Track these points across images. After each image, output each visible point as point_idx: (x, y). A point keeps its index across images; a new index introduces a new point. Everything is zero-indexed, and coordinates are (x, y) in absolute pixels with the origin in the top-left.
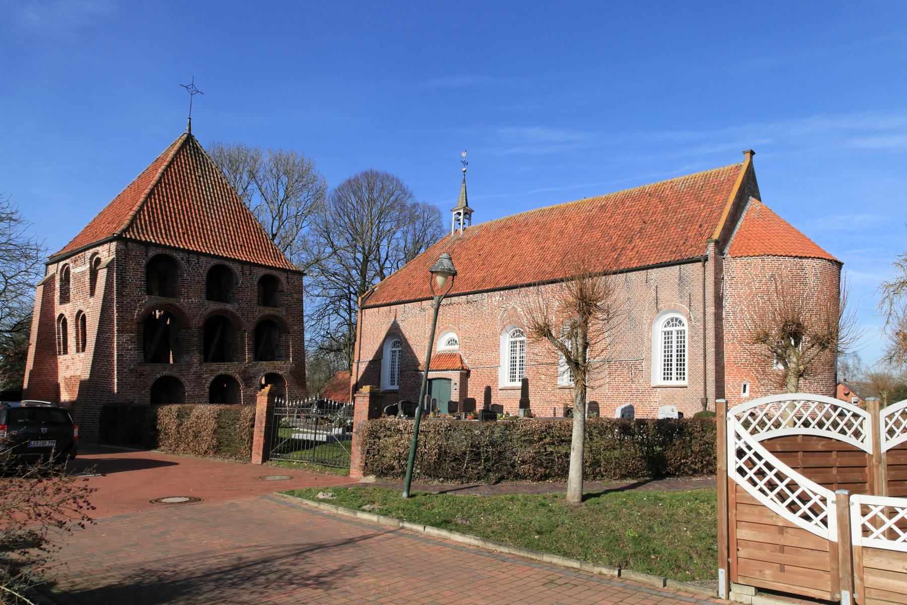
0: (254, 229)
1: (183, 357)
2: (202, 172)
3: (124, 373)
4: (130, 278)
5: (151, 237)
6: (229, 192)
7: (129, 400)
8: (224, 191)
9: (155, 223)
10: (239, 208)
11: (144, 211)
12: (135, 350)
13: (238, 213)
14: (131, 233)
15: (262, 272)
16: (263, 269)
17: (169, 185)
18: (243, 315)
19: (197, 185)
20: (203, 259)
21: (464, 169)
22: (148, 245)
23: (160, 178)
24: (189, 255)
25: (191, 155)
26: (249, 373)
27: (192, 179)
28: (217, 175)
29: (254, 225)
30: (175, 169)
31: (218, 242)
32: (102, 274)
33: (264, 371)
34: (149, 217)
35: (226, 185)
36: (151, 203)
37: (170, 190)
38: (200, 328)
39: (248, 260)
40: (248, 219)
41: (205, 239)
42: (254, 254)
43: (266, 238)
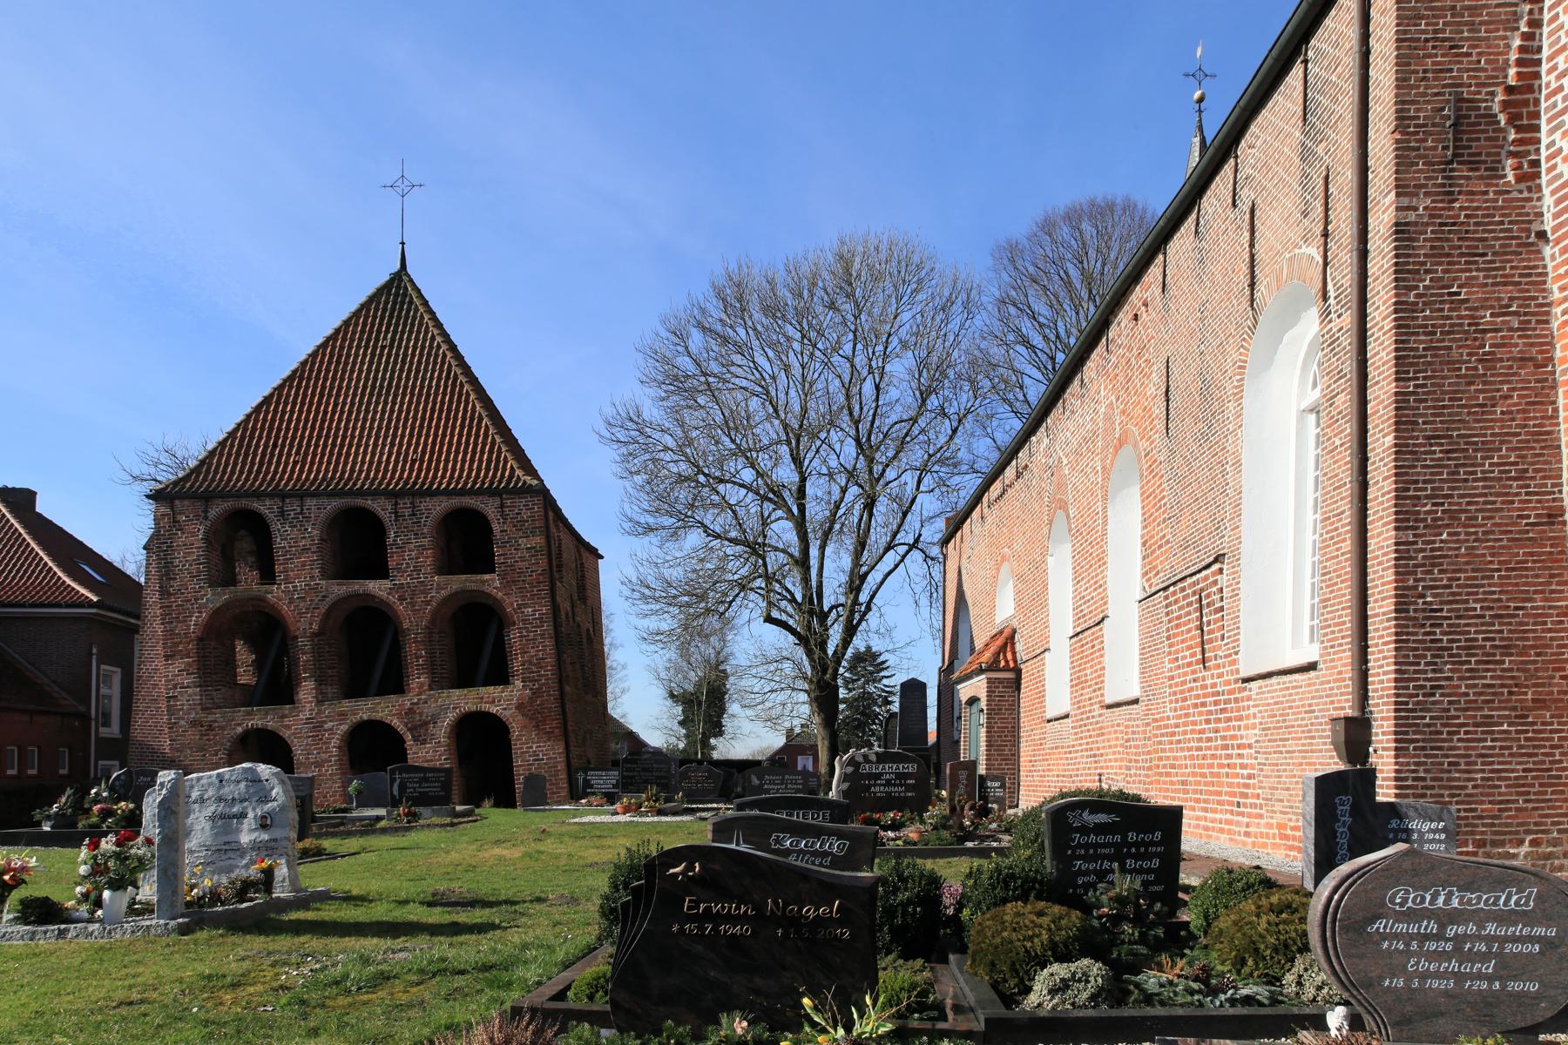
15: (439, 506)
16: (441, 498)
18: (402, 599)
21: (1197, 95)
22: (207, 498)
24: (283, 501)
33: (455, 708)
38: (314, 635)
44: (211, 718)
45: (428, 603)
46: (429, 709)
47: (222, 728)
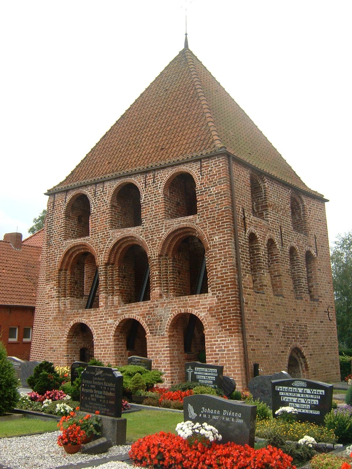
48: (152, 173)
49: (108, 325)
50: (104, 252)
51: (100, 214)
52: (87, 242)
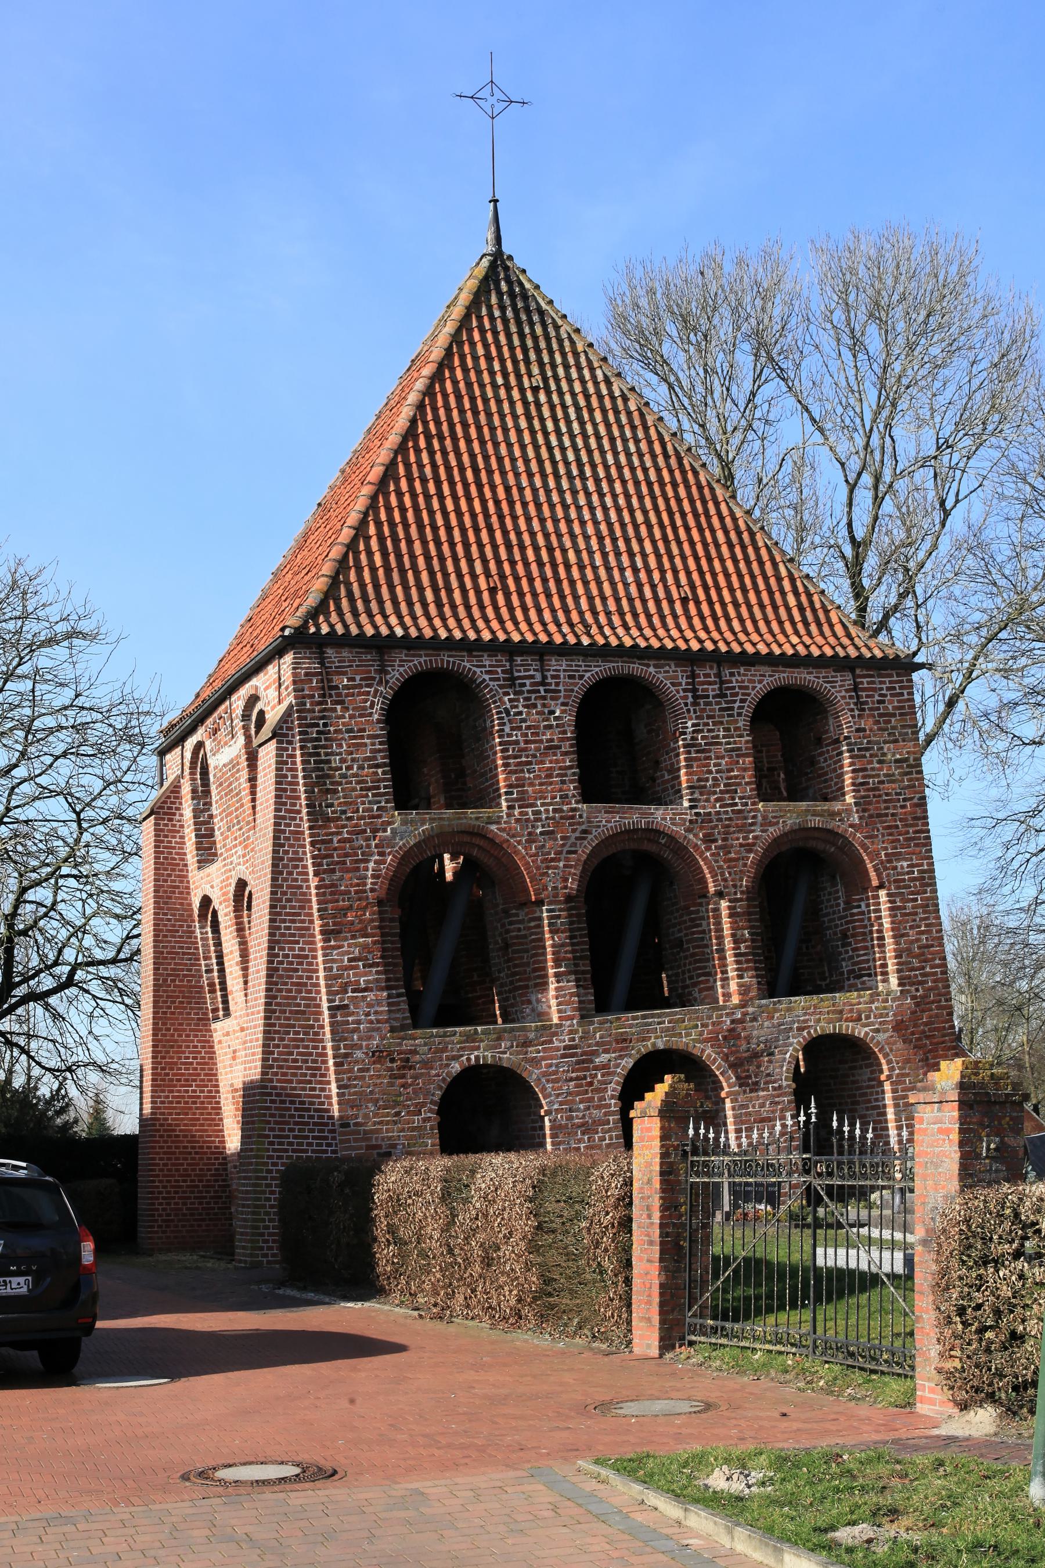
0: (726, 533)
1: (529, 1002)
2: (543, 373)
3: (357, 1062)
4: (343, 761)
5: (393, 620)
6: (637, 422)
7: (379, 1147)
8: (618, 421)
9: (403, 572)
10: (671, 472)
11: (368, 538)
12: (382, 989)
13: (669, 489)
14: (334, 618)
17: (441, 438)
18: (709, 839)
19: (529, 419)
20: (557, 665)
23: (413, 421)
24: (511, 661)
25: (505, 321)
26: (748, 1039)
27: (512, 403)
28: (592, 370)
29: (728, 521)
30: (455, 383)
31: (604, 599)
32: (268, 755)
33: (800, 1029)
34: (385, 555)
35: (625, 400)
36: (389, 510)
37: (445, 453)
38: (569, 898)
39: (709, 646)
40: (704, 503)
41: (562, 598)
42: (729, 621)
43: (772, 559)
44: (407, 1045)
45: (749, 848)
46: (760, 1031)
47: (427, 1064)
48: (711, 668)
49: (596, 1068)
50: (561, 864)
51: (538, 749)
52: (494, 827)
